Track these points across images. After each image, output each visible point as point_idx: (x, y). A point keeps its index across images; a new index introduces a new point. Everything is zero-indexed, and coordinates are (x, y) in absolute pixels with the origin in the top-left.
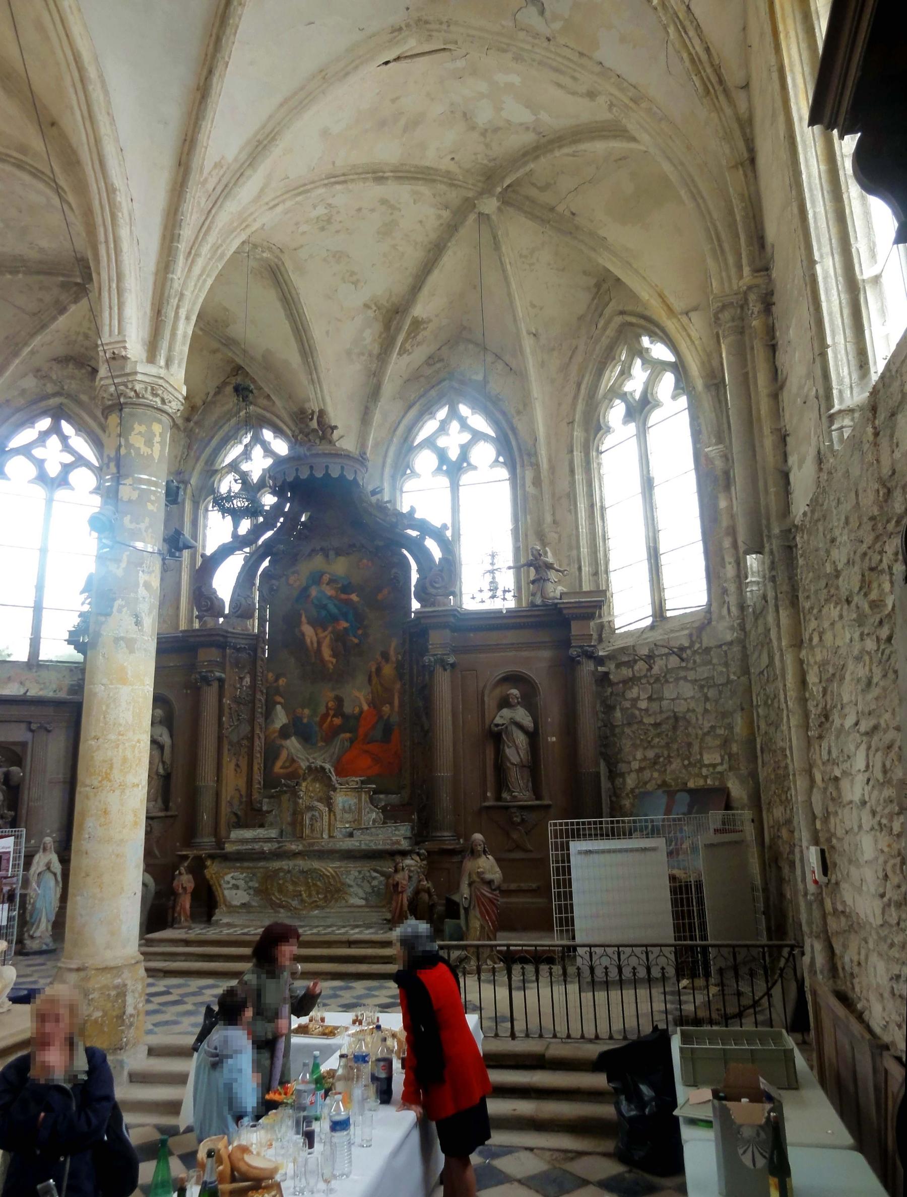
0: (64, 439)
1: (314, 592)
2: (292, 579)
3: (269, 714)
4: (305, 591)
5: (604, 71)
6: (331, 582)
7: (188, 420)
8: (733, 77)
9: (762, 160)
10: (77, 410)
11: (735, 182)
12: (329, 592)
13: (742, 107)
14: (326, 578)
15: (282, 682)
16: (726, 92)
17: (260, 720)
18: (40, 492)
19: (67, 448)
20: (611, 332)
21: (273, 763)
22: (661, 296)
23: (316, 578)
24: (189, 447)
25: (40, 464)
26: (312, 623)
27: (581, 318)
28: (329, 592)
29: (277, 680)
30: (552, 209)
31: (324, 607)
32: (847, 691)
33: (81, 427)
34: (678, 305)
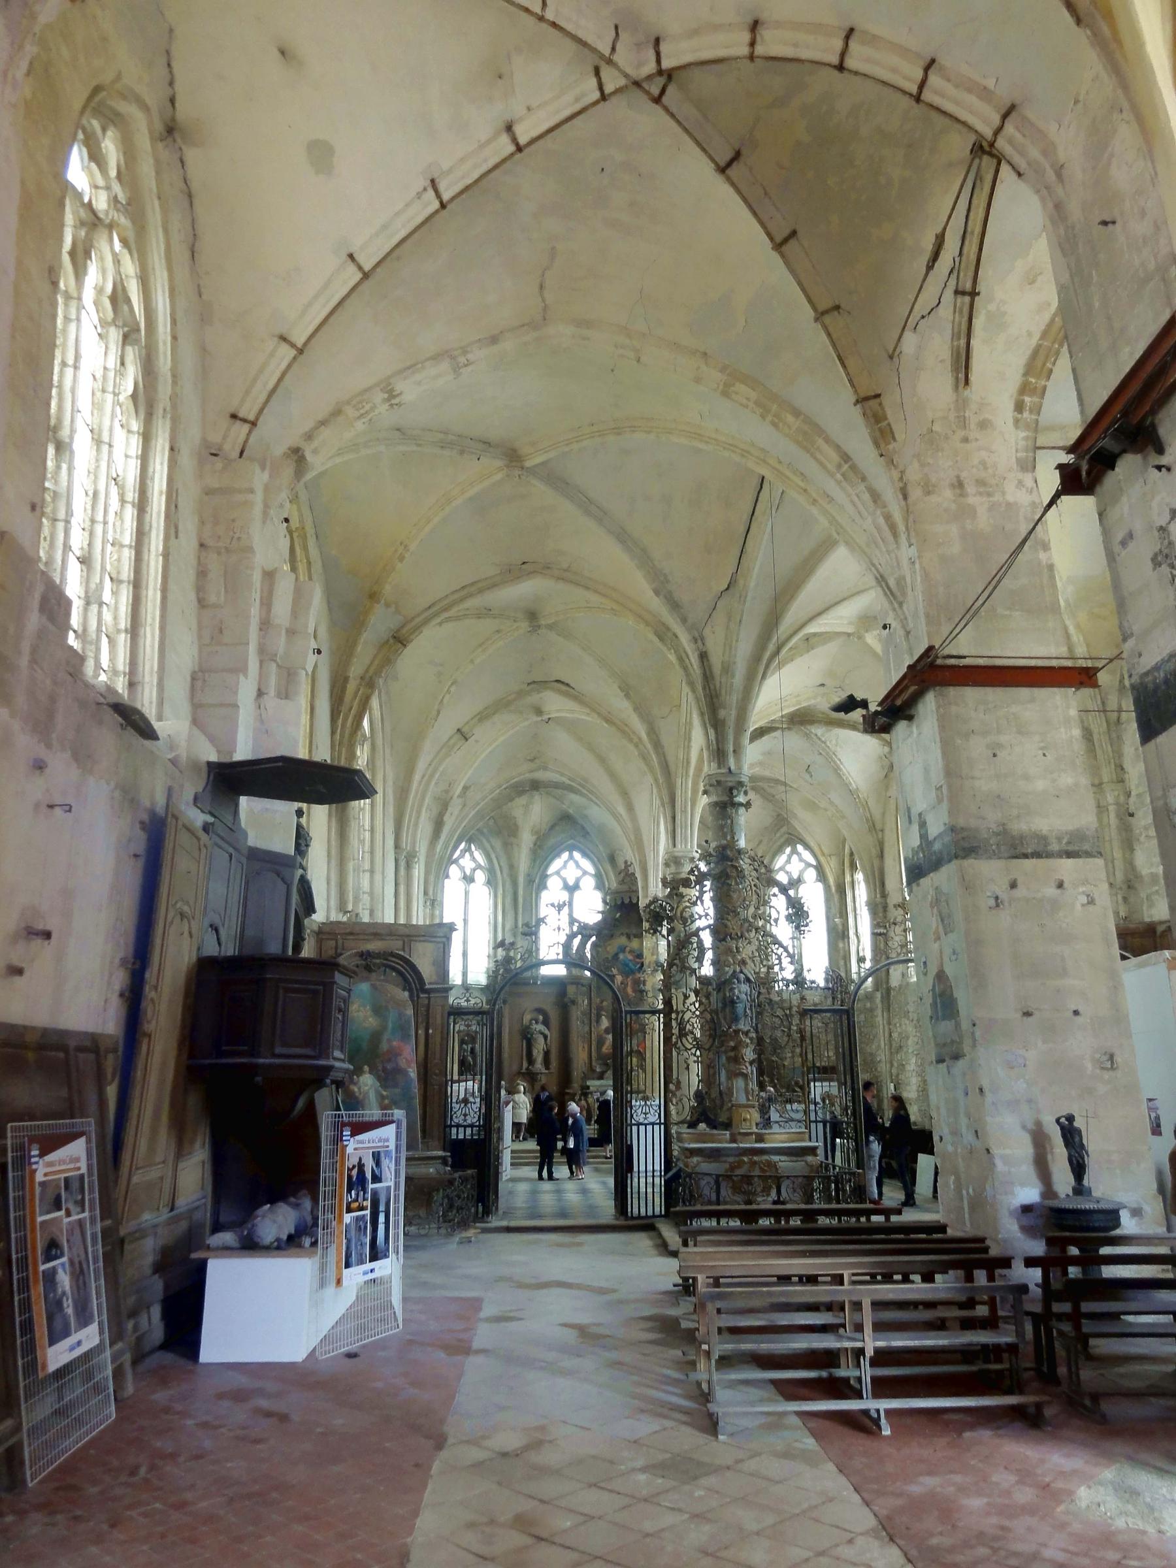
0: (472, 855)
1: (621, 956)
2: (608, 949)
3: (598, 1021)
4: (617, 954)
5: (831, 803)
6: (631, 952)
7: (535, 844)
8: (878, 826)
9: (886, 855)
10: (482, 838)
11: (876, 863)
12: (630, 957)
13: (880, 836)
14: (628, 949)
15: (605, 1003)
16: (875, 829)
17: (594, 1023)
18: (461, 885)
19: (473, 859)
20: (782, 840)
21: (601, 1048)
22: (819, 845)
23: (623, 949)
24: (534, 861)
25: (462, 869)
26: (621, 973)
27: (766, 828)
28: (630, 957)
29: (602, 1002)
30: (773, 796)
31: (627, 965)
32: (910, 1042)
33: (480, 847)
34: (826, 851)
